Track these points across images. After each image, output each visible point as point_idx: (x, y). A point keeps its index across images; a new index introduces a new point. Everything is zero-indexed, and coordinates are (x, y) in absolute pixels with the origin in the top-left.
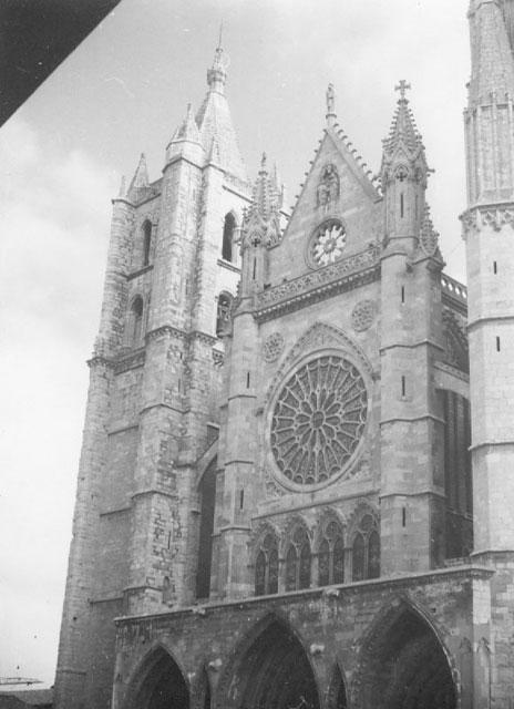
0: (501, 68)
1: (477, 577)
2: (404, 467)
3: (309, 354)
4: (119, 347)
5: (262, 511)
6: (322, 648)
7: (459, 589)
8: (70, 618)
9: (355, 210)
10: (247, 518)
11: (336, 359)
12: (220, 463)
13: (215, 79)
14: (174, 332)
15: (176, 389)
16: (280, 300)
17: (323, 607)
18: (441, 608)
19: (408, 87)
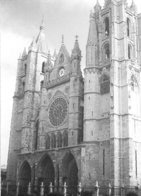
0: (93, 36)
1: (82, 147)
2: (73, 123)
3: (57, 97)
4: (20, 94)
5: (47, 131)
6: (55, 161)
7: (79, 149)
8: (10, 154)
9: (66, 65)
10: (44, 133)
11: (62, 99)
12: (40, 120)
13: (41, 29)
14: (30, 91)
15: (31, 104)
16: (51, 85)
17: (55, 153)
18: (76, 153)
19: (78, 37)
